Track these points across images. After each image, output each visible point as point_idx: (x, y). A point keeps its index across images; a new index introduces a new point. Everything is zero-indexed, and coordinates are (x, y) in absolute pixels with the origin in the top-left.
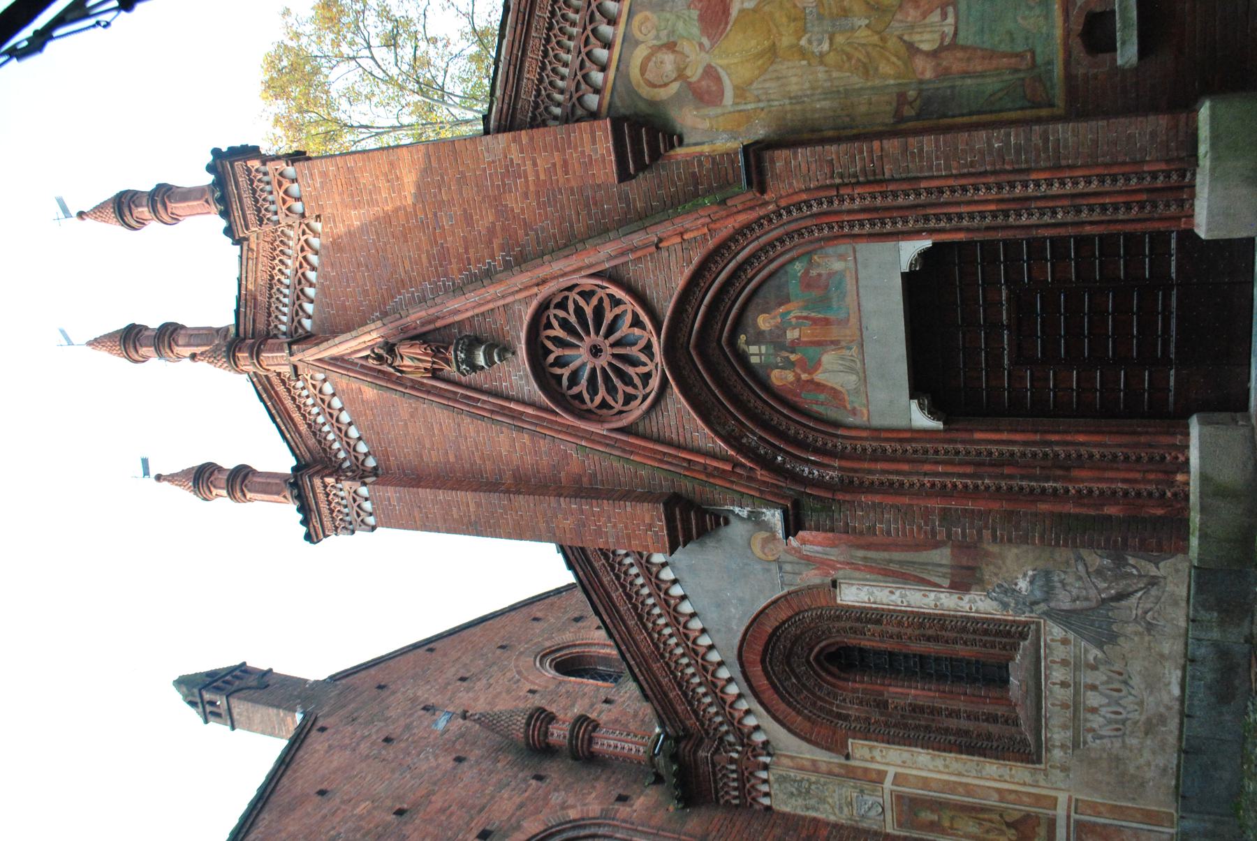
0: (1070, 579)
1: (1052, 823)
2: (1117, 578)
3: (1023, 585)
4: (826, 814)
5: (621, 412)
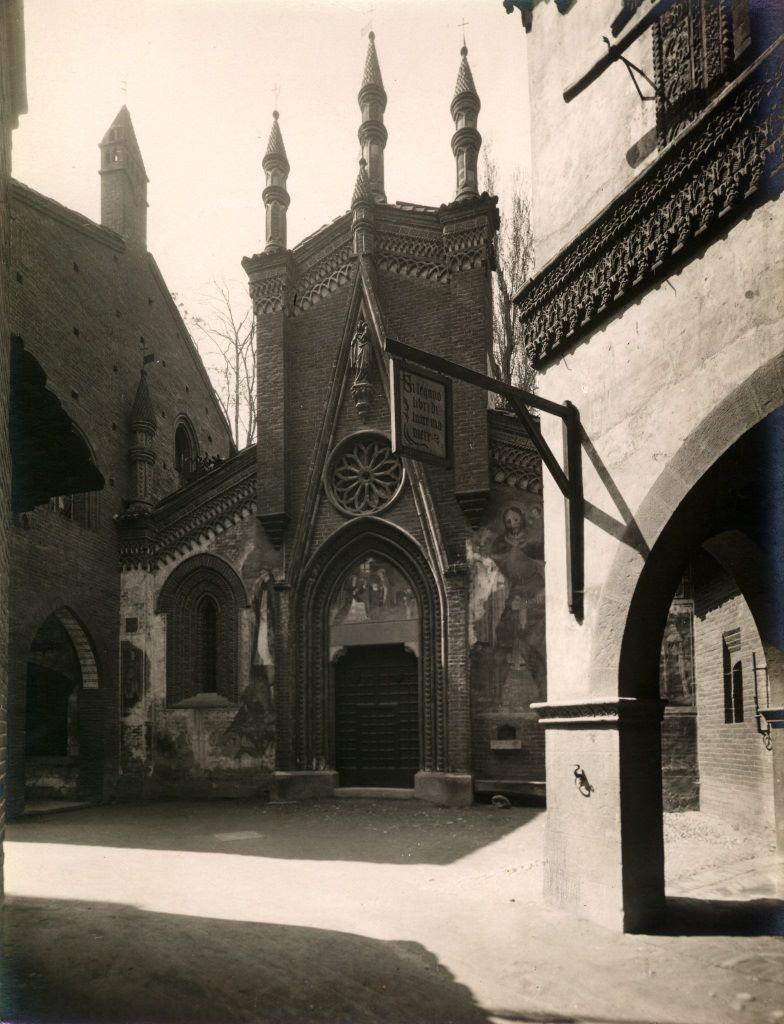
5: (333, 489)
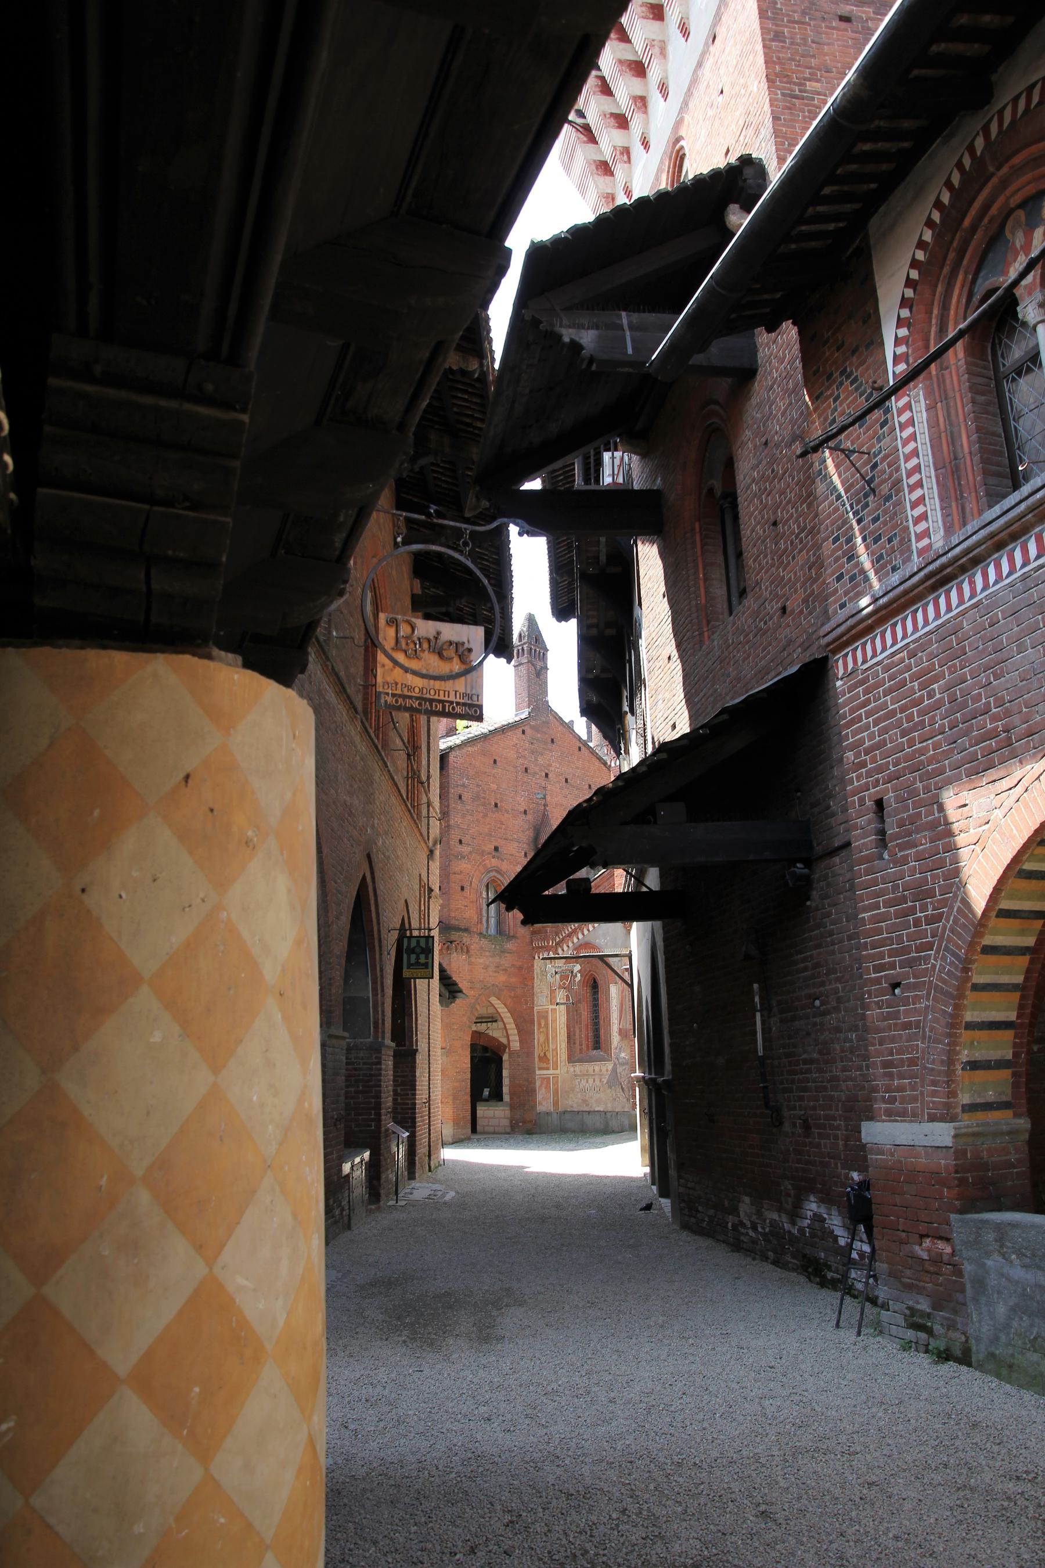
0: (626, 1072)
1: (548, 1069)
2: (628, 1088)
3: (623, 1055)
4: (536, 982)
